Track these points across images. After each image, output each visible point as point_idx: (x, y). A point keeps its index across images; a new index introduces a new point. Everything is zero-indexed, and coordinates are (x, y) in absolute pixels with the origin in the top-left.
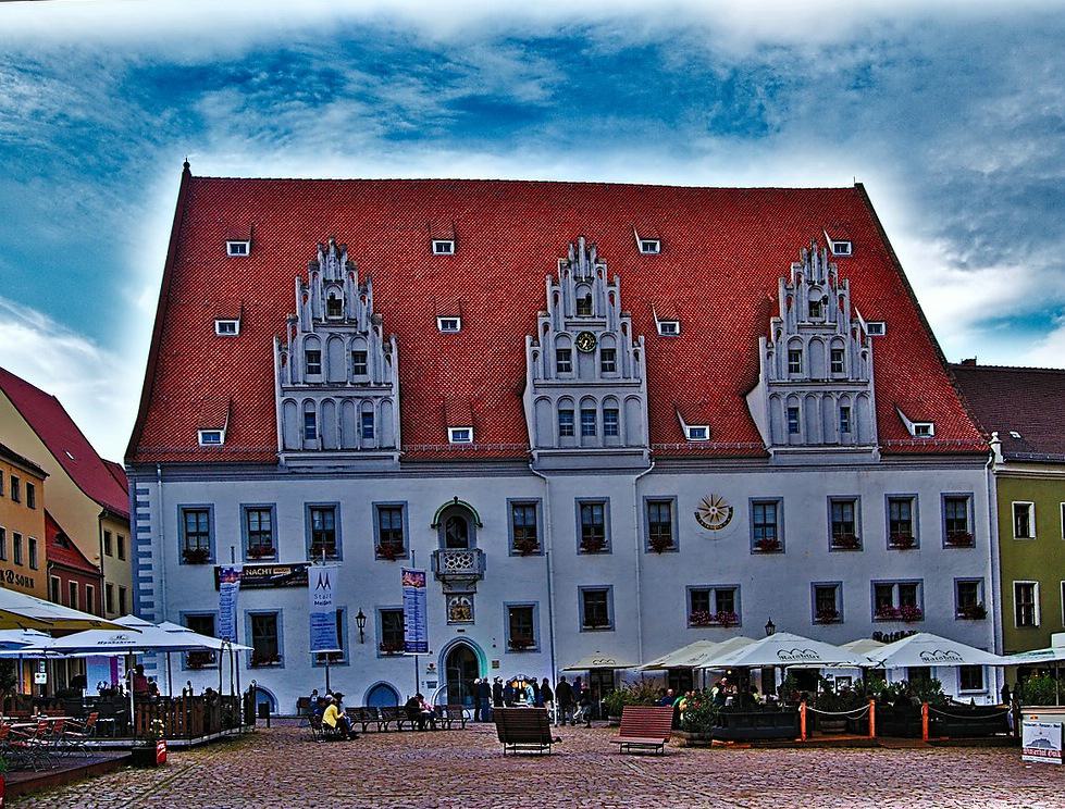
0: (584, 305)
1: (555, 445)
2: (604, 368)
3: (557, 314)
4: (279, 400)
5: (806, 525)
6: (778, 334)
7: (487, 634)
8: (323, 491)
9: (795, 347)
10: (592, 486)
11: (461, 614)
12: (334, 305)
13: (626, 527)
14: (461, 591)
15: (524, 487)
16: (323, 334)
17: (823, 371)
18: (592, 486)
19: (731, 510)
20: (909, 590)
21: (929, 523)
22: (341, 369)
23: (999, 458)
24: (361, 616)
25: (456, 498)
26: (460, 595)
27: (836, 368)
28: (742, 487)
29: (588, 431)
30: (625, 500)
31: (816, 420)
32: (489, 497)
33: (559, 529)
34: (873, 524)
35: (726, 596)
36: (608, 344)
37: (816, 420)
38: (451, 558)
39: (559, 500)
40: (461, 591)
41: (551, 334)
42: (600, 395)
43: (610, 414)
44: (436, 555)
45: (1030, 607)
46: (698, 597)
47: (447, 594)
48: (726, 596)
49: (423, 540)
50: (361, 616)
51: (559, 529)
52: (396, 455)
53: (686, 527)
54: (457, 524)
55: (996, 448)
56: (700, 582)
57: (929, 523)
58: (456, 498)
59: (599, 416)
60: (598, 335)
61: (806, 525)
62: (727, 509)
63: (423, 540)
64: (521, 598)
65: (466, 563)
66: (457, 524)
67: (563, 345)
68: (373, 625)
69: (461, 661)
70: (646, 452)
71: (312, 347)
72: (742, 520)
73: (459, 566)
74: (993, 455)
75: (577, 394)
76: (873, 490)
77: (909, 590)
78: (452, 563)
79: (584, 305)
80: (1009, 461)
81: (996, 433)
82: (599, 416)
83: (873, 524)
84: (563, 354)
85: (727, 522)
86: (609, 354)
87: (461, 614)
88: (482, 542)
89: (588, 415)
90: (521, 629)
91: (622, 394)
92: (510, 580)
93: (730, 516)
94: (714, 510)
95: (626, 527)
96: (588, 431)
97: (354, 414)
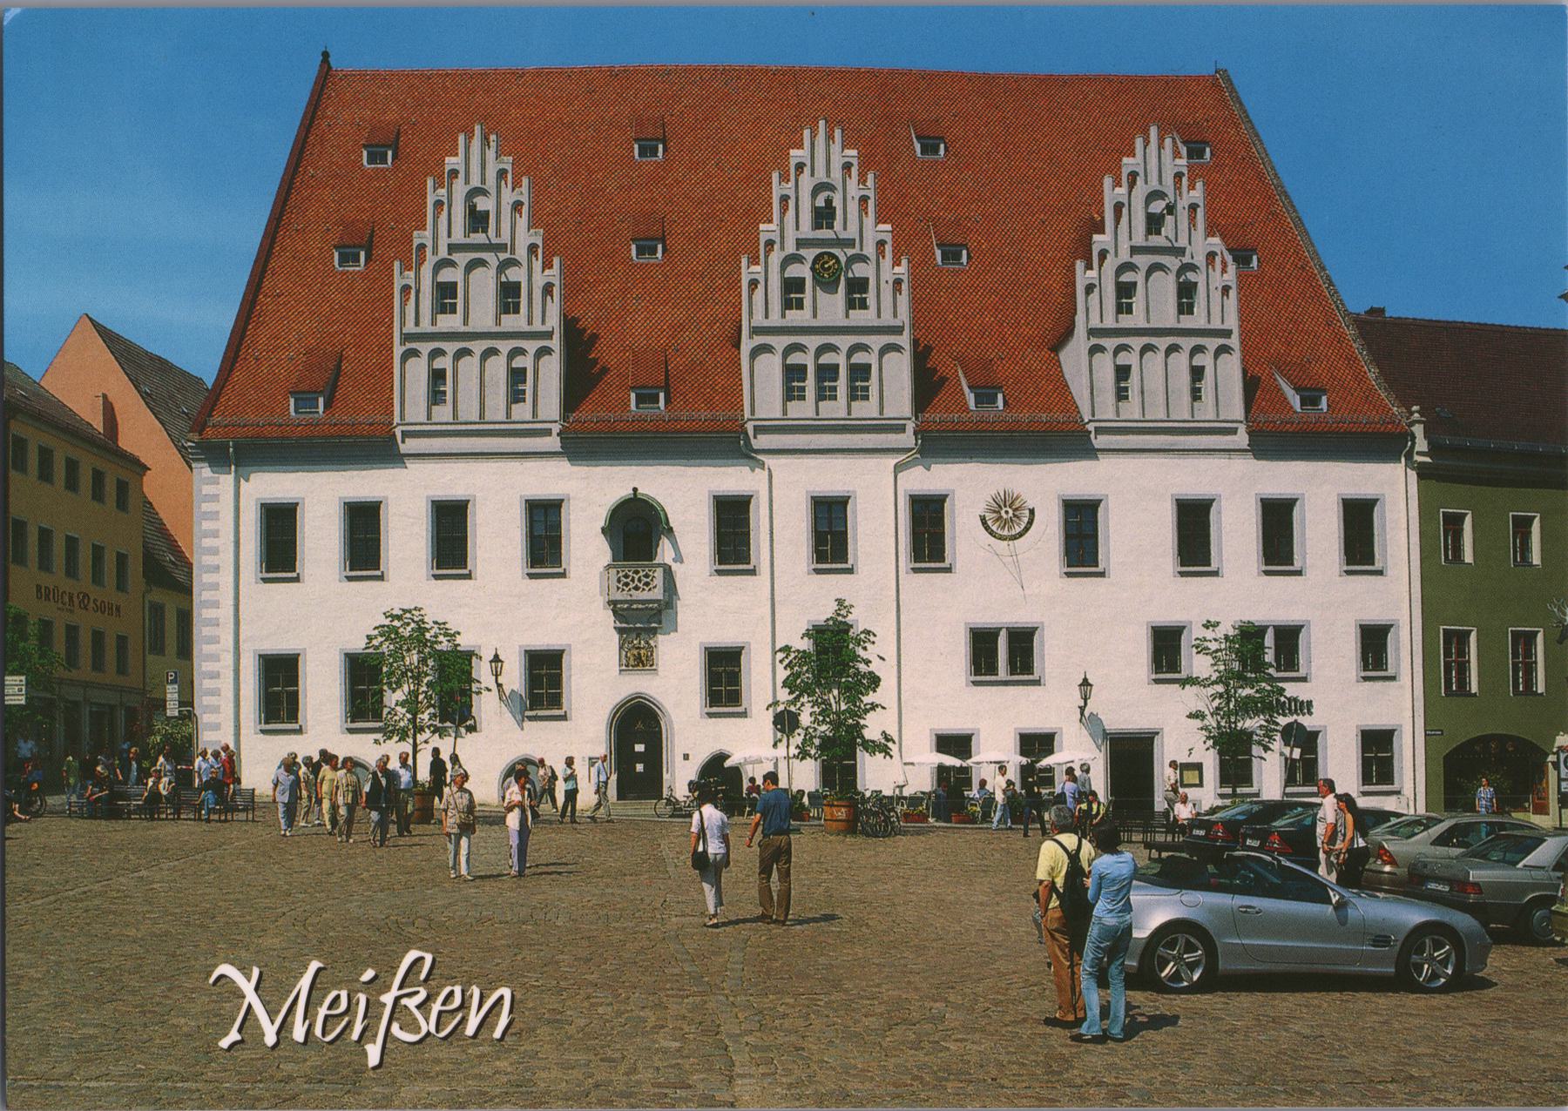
0: (824, 216)
1: (779, 415)
2: (851, 304)
3: (787, 228)
4: (398, 351)
5: (1138, 530)
6: (1103, 255)
7: (675, 682)
8: (451, 481)
9: (1127, 277)
10: (830, 476)
11: (638, 658)
12: (477, 220)
13: (878, 531)
14: (640, 625)
15: (732, 479)
16: (462, 259)
17: (1166, 315)
18: (830, 476)
19: (1032, 512)
20: (1288, 637)
21: (1319, 533)
22: (482, 309)
23: (1421, 444)
24: (496, 659)
25: (635, 490)
26: (638, 633)
27: (1185, 308)
28: (1044, 484)
29: (824, 394)
30: (877, 493)
31: (1155, 381)
32: (684, 492)
33: (783, 531)
34: (1237, 534)
35: (1023, 642)
36: (859, 270)
37: (1155, 381)
38: (626, 576)
39: (783, 491)
40: (640, 625)
41: (776, 258)
42: (845, 342)
43: (860, 373)
44: (608, 567)
45: (1463, 668)
47: (620, 631)
48: (1023, 642)
49: (586, 544)
50: (496, 659)
51: (783, 531)
52: (556, 428)
53: (964, 530)
54: (636, 529)
55: (1418, 430)
56: (986, 620)
57: (1319, 533)
58: (635, 490)
59: (843, 372)
60: (843, 260)
61: (1138, 530)
62: (1027, 512)
63: (586, 544)
64: (725, 637)
65: (647, 584)
66: (636, 529)
67: (794, 271)
68: (515, 677)
69: (637, 726)
70: (910, 426)
71: (446, 275)
72: (1049, 530)
73: (637, 588)
74: (1413, 438)
75: (813, 342)
76: (1237, 486)
77: (1288, 637)
78: (627, 584)
79: (824, 216)
80: (1433, 450)
81: (1415, 408)
82: (843, 372)
83: (1237, 534)
84: (792, 287)
85: (1027, 529)
86: (858, 287)
87: (638, 658)
88: (665, 552)
89: (827, 373)
90: (723, 675)
91: (876, 342)
92: (710, 608)
93: (1030, 522)
94: (1006, 513)
95: (878, 531)
96: (824, 394)
97: (498, 368)
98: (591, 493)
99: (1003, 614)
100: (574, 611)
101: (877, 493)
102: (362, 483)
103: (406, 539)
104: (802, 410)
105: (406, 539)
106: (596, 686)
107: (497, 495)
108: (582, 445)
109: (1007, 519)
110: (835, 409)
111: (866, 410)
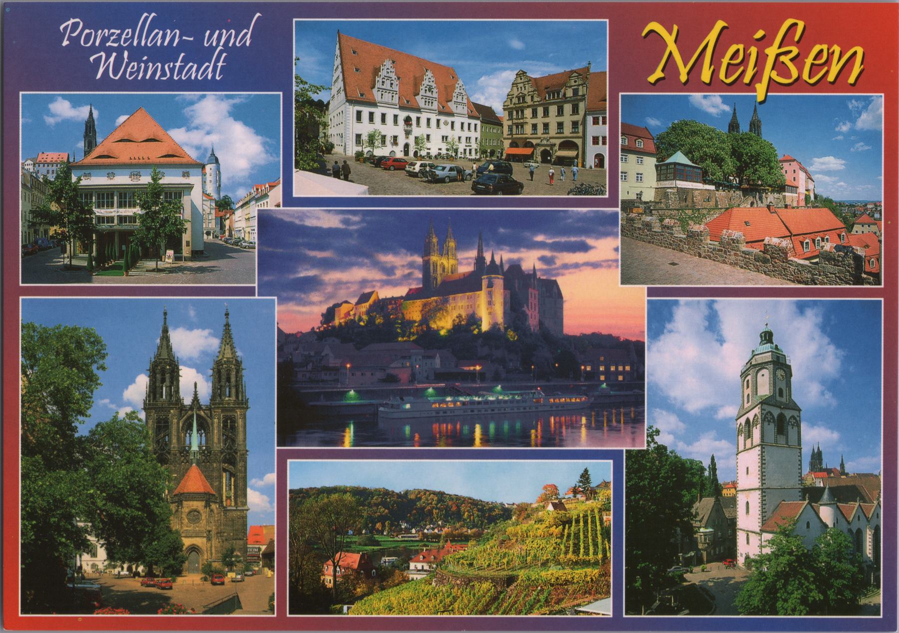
13: (433, 123)
15: (419, 115)
30: (434, 118)
32: (414, 116)
33: (423, 122)
39: (424, 116)
40: (408, 133)
46: (443, 137)
95: (433, 123)
98: (402, 115)
99: (445, 135)
100: (399, 131)
101: (434, 118)
102: (372, 110)
103: (377, 118)
104: (427, 106)
105: (377, 118)
106: (402, 141)
107: (390, 113)
108: (402, 108)
109: (446, 123)
110: (430, 107)
111: (433, 108)
